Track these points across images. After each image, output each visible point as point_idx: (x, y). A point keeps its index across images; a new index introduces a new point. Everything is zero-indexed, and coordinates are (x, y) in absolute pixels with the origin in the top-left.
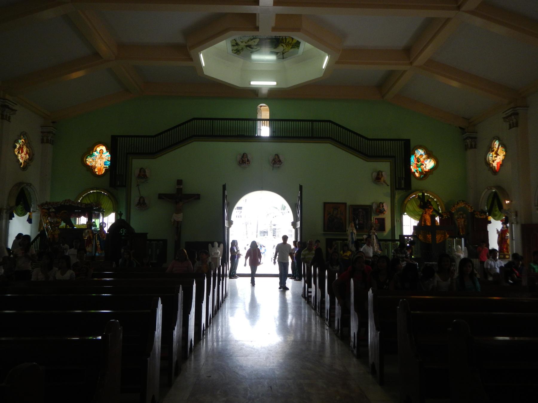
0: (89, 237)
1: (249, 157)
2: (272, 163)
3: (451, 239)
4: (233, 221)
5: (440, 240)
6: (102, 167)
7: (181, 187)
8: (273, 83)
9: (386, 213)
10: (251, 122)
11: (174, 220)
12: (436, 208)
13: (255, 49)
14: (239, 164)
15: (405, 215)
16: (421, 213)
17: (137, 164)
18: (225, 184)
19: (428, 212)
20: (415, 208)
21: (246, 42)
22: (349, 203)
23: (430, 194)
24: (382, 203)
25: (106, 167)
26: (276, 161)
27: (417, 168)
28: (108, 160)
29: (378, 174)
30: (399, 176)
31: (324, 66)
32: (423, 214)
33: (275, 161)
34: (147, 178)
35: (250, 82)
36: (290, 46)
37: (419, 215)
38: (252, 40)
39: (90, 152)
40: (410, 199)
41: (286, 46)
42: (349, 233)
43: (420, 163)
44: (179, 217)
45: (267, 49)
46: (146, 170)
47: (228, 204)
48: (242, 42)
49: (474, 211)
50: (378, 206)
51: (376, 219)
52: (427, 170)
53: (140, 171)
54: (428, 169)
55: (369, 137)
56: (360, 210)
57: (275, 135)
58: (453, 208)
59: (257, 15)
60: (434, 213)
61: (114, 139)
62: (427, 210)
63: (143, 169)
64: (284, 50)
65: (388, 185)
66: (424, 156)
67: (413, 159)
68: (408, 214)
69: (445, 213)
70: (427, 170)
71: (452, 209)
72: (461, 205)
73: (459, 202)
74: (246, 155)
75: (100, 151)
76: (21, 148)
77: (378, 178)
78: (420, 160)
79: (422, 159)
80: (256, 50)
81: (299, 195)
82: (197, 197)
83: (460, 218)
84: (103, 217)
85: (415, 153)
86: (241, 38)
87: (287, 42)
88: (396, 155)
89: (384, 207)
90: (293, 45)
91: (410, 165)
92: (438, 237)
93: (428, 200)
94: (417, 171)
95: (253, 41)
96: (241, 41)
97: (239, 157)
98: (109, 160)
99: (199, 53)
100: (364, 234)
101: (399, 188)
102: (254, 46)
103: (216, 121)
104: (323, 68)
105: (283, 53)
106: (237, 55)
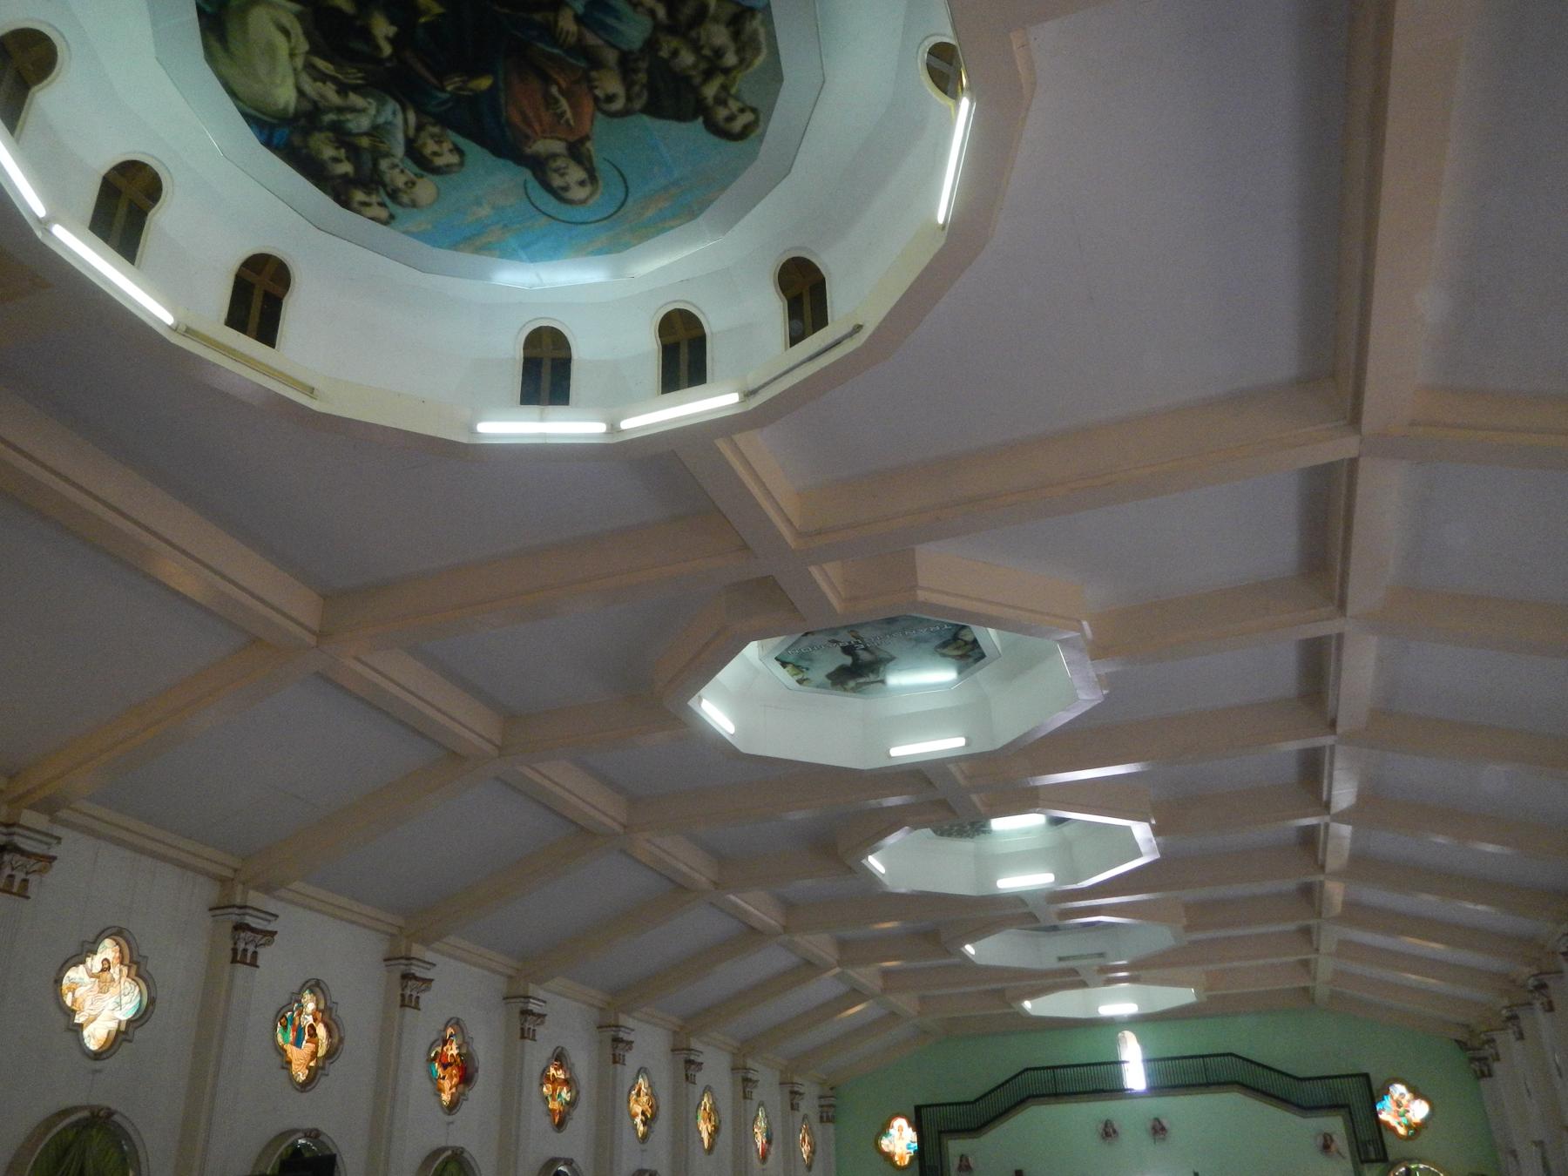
1: (1116, 1126)
17: (956, 1147)
26: (1158, 1129)
29: (1326, 1140)
39: (884, 1129)
53: (961, 1161)
55: (1300, 1076)
61: (918, 1109)
65: (1344, 1158)
76: (804, 1138)
77: (1326, 1147)
79: (1404, 1102)
94: (1399, 1123)
97: (1101, 1126)
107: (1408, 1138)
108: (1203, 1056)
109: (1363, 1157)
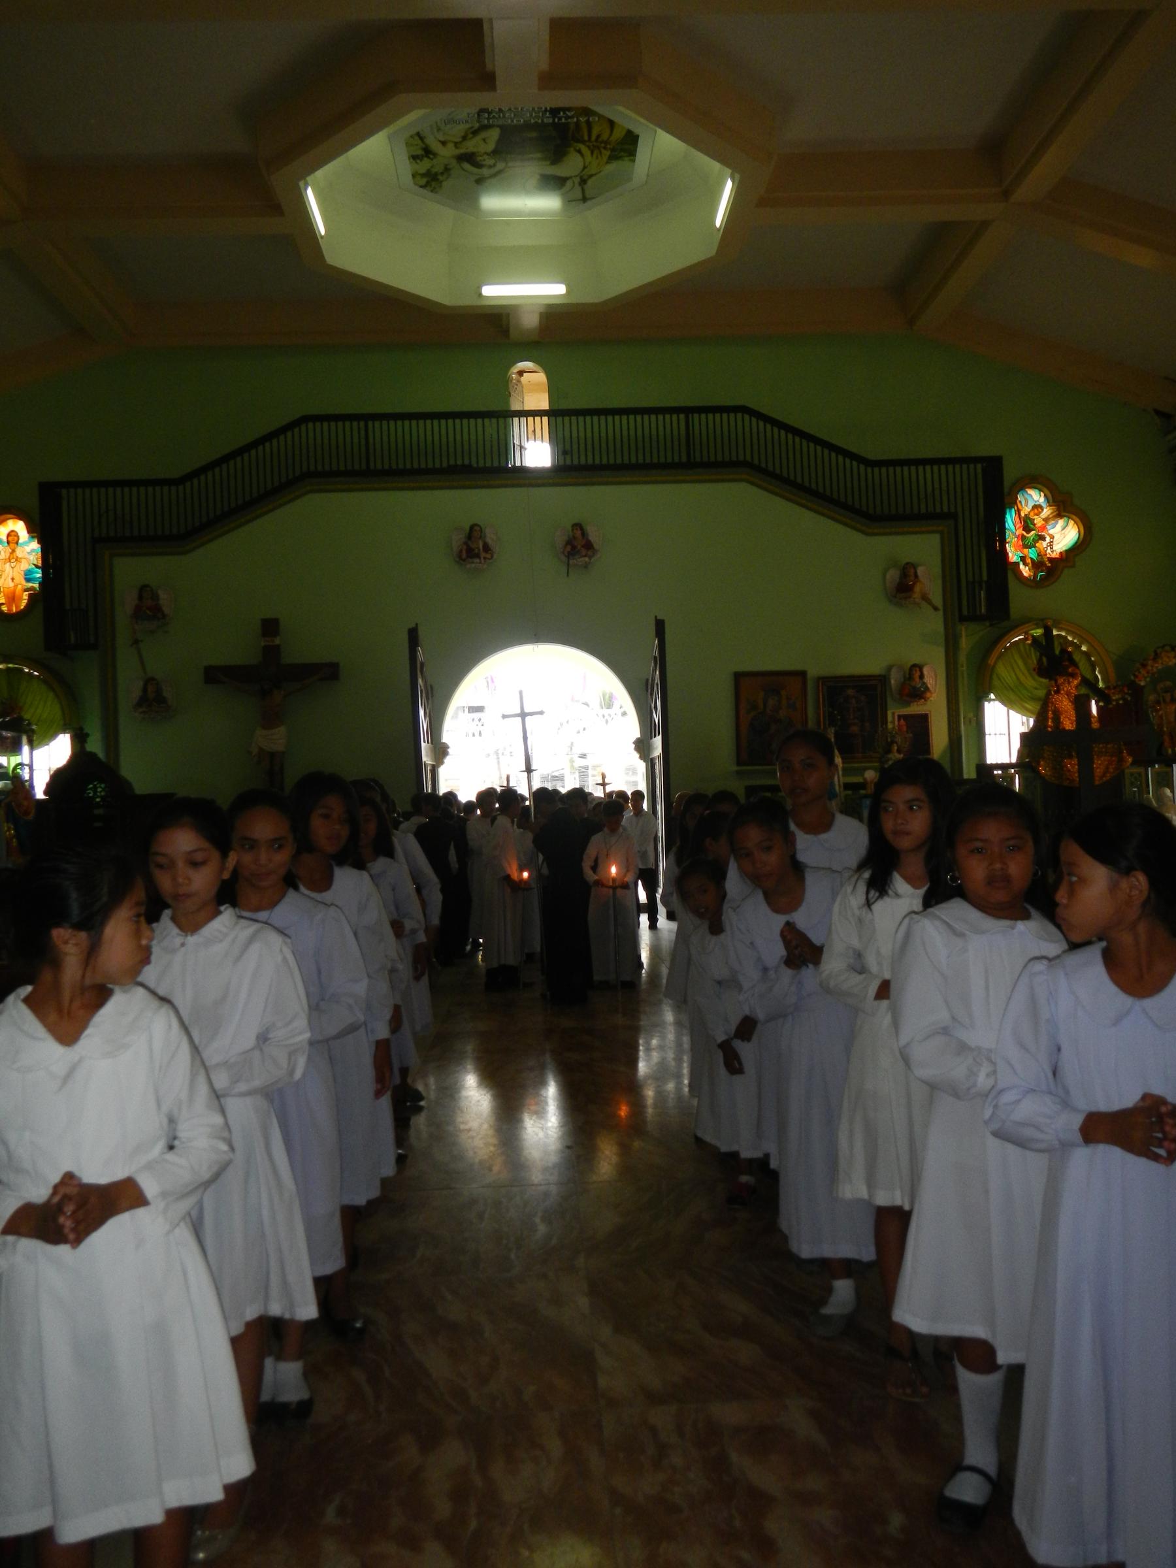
1: (490, 538)
2: (563, 553)
3: (1141, 770)
4: (450, 745)
5: (1104, 775)
6: (20, 587)
7: (277, 641)
8: (556, 290)
9: (932, 699)
10: (490, 425)
11: (261, 749)
12: (1089, 676)
13: (490, 167)
14: (458, 560)
15: (992, 702)
16: (1041, 693)
18: (414, 626)
19: (1066, 687)
20: (1022, 678)
21: (456, 145)
22: (813, 672)
23: (1069, 632)
24: (919, 667)
25: (32, 589)
27: (1026, 551)
28: (37, 566)
30: (970, 579)
31: (719, 221)
32: (1048, 693)
33: (574, 547)
34: (164, 616)
35: (479, 288)
36: (603, 151)
37: (1033, 699)
38: (475, 133)
40: (1006, 649)
41: (592, 153)
43: (1033, 533)
44: (276, 739)
45: (530, 168)
46: (160, 592)
47: (430, 692)
48: (444, 143)
50: (907, 676)
51: (899, 717)
52: (1054, 555)
53: (140, 598)
54: (1059, 551)
55: (871, 456)
56: (850, 692)
57: (568, 462)
58: (1143, 672)
59: (486, 26)
60: (1083, 691)
62: (1061, 680)
63: (148, 589)
64: (585, 168)
65: (936, 609)
66: (1045, 510)
67: (1011, 521)
69: (1115, 688)
70: (1057, 556)
71: (1137, 673)
72: (1165, 659)
73: (1159, 651)
74: (481, 530)
75: (8, 535)
78: (1034, 525)
79: (1038, 521)
80: (493, 171)
81: (656, 652)
82: (329, 672)
83: (1164, 701)
84: (32, 748)
85: (1016, 503)
86: (439, 129)
87: (594, 138)
88: (959, 510)
89: (926, 680)
90: (613, 150)
91: (1003, 542)
92: (1100, 765)
93: (1064, 651)
95: (478, 138)
96: (442, 139)
97: (458, 540)
98: (40, 564)
99: (301, 184)
100: (865, 769)
101: (973, 618)
102: (486, 157)
103: (377, 424)
104: (718, 224)
105: (583, 182)
106: (432, 191)
107: (1032, 583)
108: (688, 411)
109: (965, 612)
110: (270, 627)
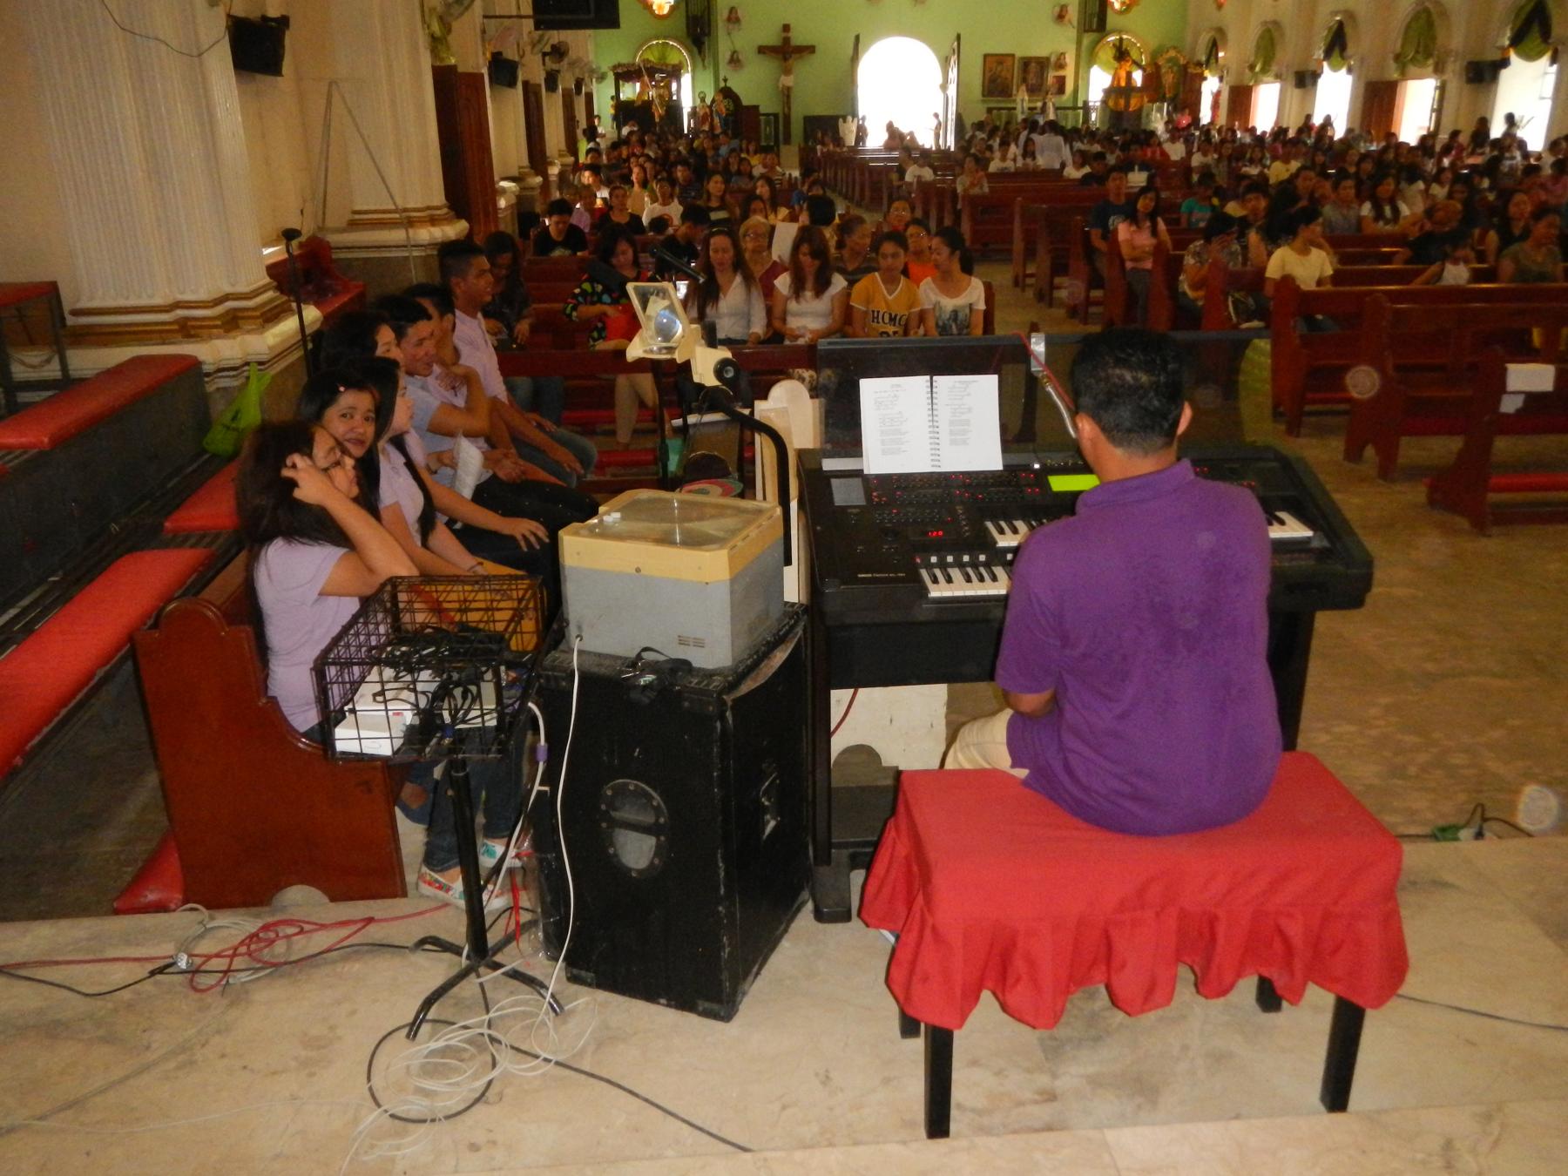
0: (706, 113)
29: (1061, 11)
42: (1018, 99)
44: (788, 81)
49: (1188, 63)
68: (1100, 66)
77: (1061, 17)
82: (811, 49)
93: (1126, 50)
107: (1121, 13)
110: (786, 28)
